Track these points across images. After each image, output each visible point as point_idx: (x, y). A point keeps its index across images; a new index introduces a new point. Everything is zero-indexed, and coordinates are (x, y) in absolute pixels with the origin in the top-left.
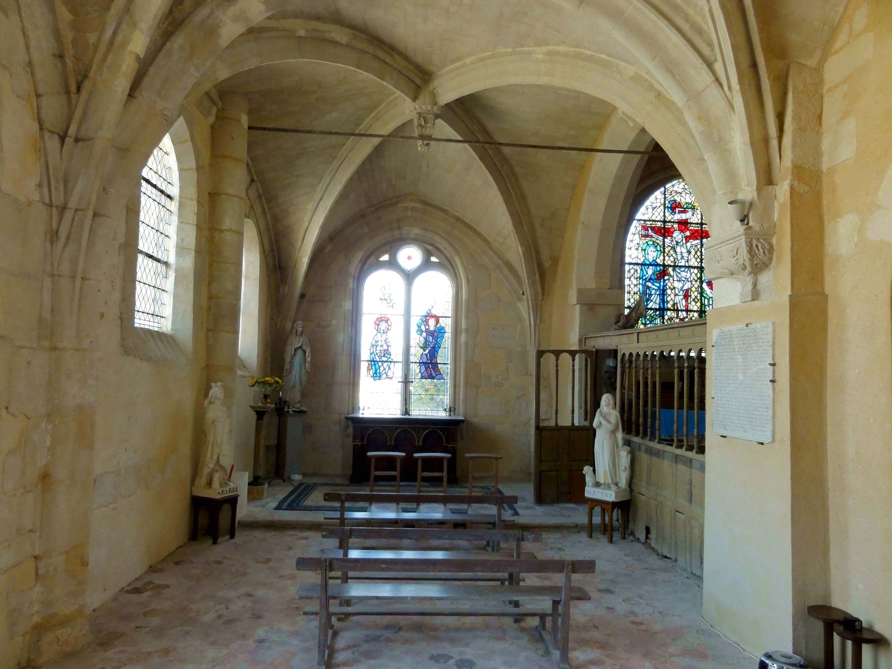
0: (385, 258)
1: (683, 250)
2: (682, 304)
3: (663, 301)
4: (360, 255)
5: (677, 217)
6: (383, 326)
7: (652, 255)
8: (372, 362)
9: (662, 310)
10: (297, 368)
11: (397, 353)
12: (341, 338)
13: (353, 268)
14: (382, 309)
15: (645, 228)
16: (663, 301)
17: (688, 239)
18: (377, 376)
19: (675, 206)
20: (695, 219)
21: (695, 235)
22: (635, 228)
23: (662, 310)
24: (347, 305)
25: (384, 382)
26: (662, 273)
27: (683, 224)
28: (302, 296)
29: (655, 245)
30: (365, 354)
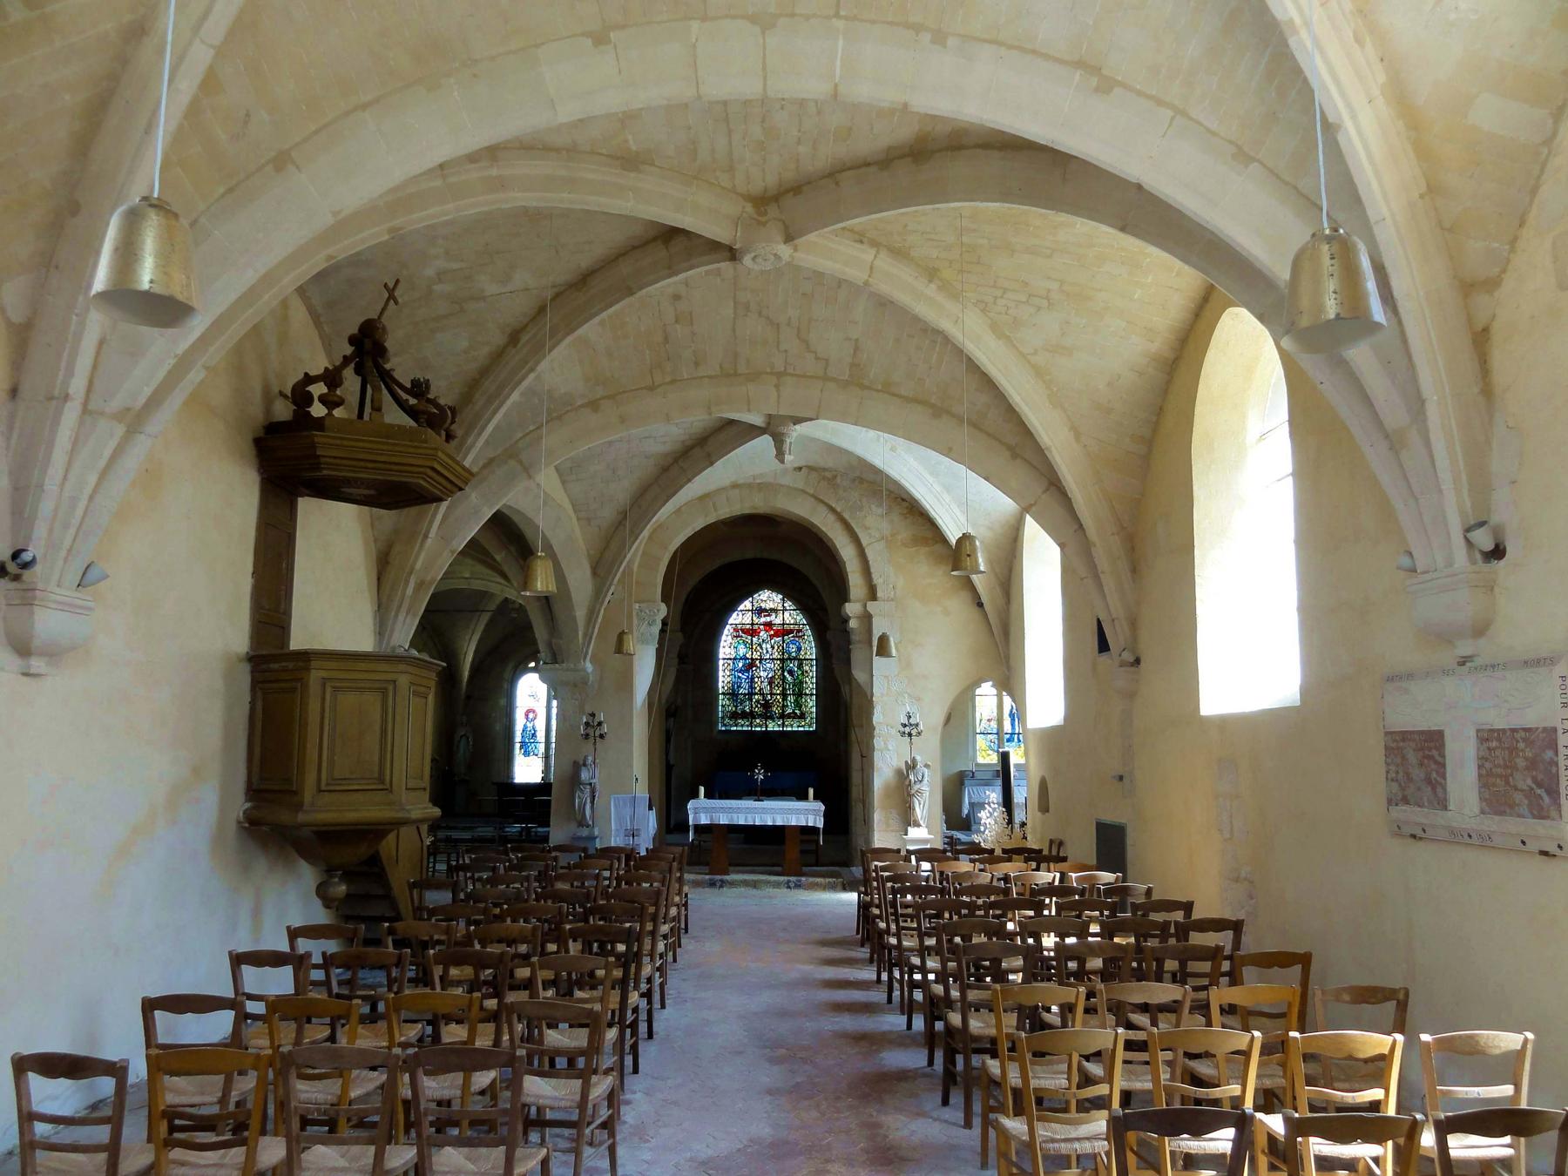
0: (532, 664)
1: (769, 647)
2: (767, 690)
3: (751, 687)
4: (511, 666)
5: (763, 620)
6: (531, 716)
7: (742, 651)
8: (523, 744)
9: (751, 694)
10: (463, 751)
11: (541, 736)
12: (498, 727)
13: (507, 675)
14: (531, 704)
15: (736, 630)
16: (751, 687)
17: (772, 637)
18: (526, 754)
19: (760, 611)
20: (778, 621)
21: (777, 634)
22: (727, 631)
23: (751, 694)
24: (503, 702)
25: (532, 758)
26: (750, 665)
27: (769, 625)
28: (468, 697)
29: (745, 643)
30: (518, 738)
